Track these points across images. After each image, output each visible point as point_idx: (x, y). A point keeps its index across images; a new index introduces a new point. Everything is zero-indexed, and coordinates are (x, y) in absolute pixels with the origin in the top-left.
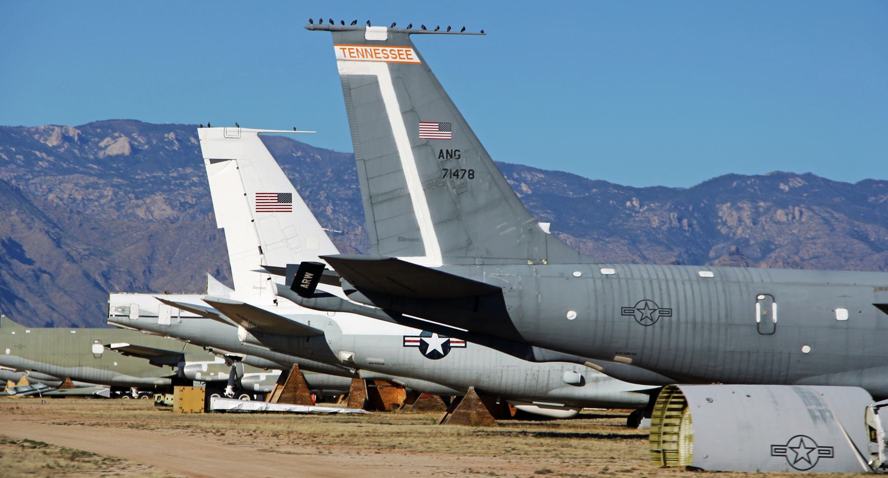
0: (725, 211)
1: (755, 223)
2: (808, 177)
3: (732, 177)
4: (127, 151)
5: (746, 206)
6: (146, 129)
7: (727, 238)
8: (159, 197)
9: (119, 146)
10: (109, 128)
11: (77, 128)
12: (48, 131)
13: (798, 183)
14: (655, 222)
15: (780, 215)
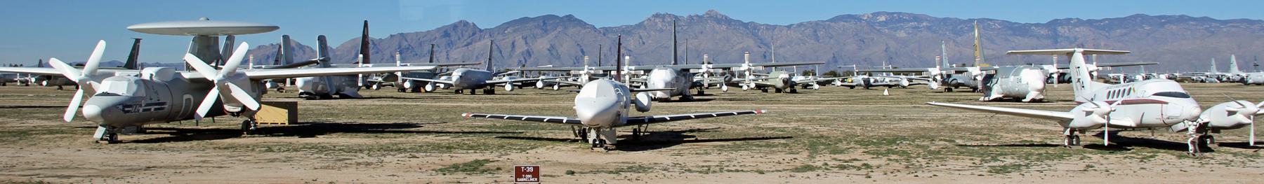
0: (1059, 29)
1: (1069, 31)
2: (1077, 19)
3: (1056, 20)
4: (885, 20)
5: (1066, 27)
6: (888, 14)
7: (1062, 36)
8: (902, 31)
9: (882, 19)
10: (879, 14)
11: (872, 14)
12: (864, 16)
13: (1076, 21)
14: (1042, 32)
15: (1077, 29)
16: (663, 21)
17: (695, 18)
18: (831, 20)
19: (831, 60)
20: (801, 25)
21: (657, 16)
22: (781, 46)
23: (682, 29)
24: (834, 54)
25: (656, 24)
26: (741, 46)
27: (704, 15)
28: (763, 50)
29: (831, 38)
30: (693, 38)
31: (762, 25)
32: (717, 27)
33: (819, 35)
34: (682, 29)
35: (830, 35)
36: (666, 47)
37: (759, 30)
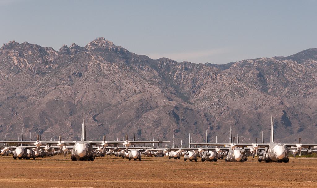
16: (20, 55)
17: (73, 51)
18: (293, 58)
19: (279, 121)
20: (244, 63)
21: (12, 46)
22: (205, 98)
23: (50, 67)
24: (284, 111)
25: (10, 59)
26: (137, 97)
27: (87, 46)
28: (174, 103)
29: (286, 86)
30: (65, 84)
31: (180, 64)
32: (105, 67)
33: (268, 80)
34: (50, 67)
35: (285, 82)
36: (23, 97)
37: (174, 72)
